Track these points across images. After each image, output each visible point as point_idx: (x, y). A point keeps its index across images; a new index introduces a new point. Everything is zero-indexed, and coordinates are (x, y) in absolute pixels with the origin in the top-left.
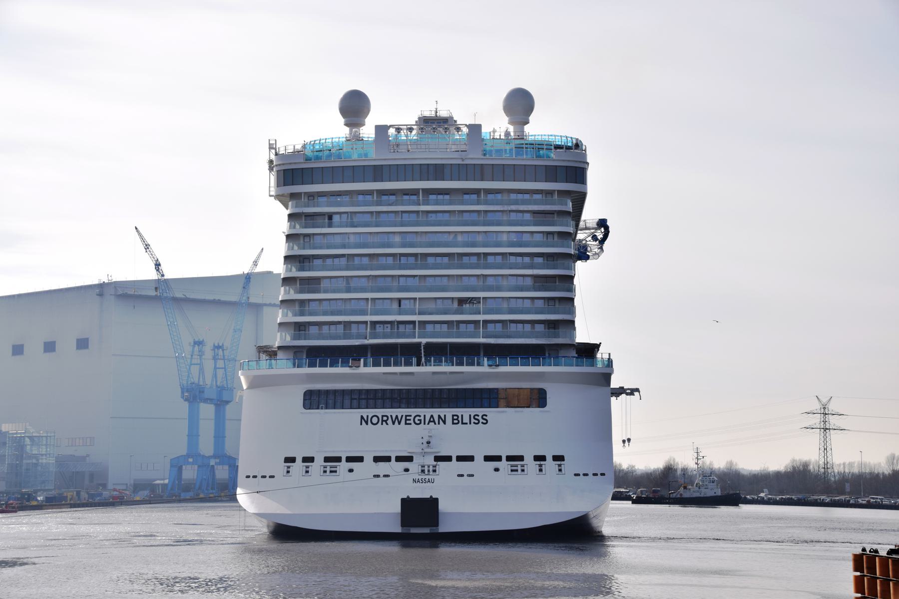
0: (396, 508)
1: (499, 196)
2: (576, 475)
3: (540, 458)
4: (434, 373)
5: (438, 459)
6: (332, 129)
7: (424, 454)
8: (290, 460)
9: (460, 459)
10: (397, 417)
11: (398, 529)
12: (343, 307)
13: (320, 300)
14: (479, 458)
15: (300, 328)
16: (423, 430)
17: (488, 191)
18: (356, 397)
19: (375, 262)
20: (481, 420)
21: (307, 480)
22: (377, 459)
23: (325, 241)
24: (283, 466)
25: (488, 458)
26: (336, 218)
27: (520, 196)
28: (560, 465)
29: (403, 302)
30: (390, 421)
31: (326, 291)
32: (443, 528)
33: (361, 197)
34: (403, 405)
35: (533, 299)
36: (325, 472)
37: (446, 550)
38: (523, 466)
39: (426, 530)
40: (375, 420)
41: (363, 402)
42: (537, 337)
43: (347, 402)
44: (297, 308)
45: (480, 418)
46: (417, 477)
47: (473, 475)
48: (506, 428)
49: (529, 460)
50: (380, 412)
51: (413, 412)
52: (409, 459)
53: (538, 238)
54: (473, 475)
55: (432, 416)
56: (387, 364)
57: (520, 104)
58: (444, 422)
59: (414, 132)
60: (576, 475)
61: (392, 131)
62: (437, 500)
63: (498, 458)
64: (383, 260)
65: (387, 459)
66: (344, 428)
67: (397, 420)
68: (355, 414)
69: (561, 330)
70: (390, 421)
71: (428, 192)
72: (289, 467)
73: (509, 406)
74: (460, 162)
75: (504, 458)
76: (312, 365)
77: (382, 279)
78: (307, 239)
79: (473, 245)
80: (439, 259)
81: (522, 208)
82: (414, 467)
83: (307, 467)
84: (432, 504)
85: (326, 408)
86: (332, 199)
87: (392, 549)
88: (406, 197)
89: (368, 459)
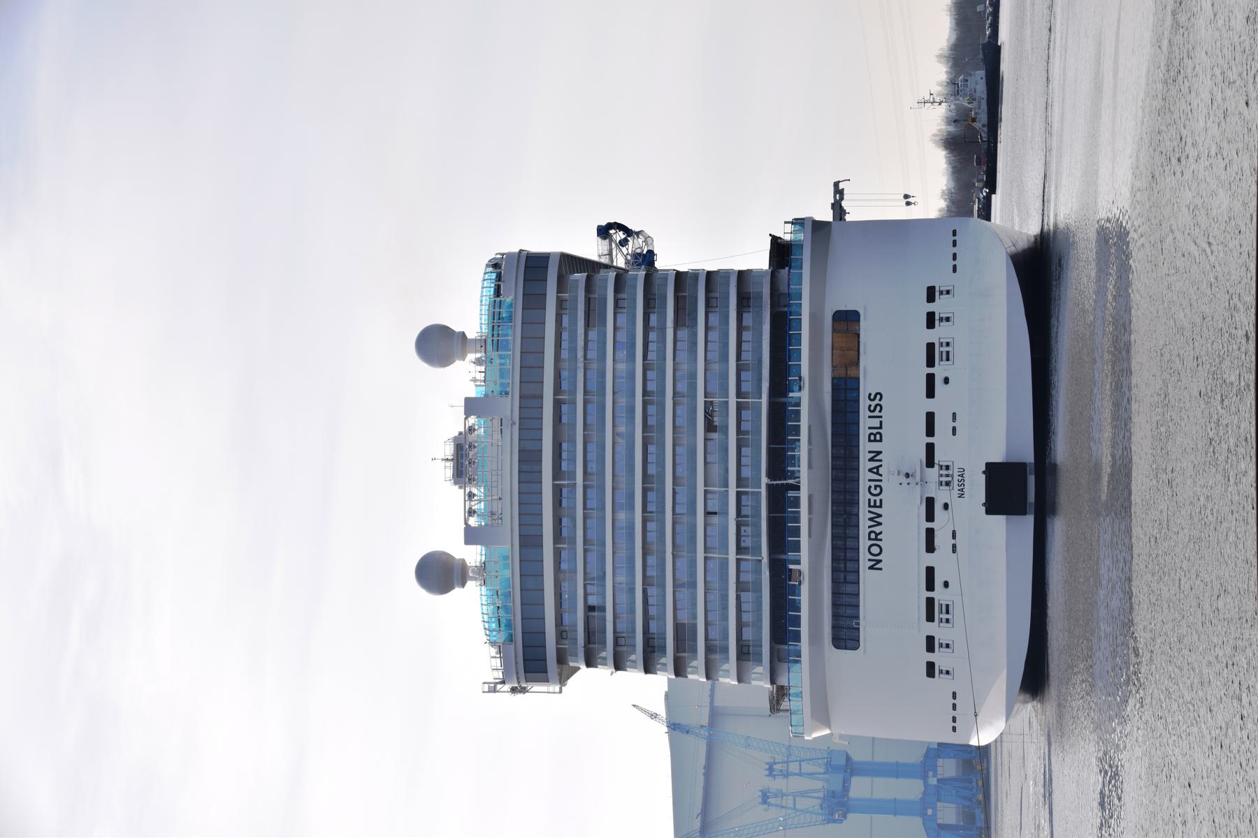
0: (1000, 520)
1: (565, 374)
2: (955, 269)
3: (931, 321)
4: (810, 467)
5: (930, 462)
6: (469, 605)
7: (924, 482)
8: (931, 669)
9: (930, 431)
10: (871, 519)
11: (1029, 521)
12: (715, 590)
13: (707, 624)
14: (930, 405)
15: (745, 653)
16: (890, 483)
17: (558, 389)
18: (842, 575)
19: (654, 548)
20: (877, 401)
21: (959, 646)
22: (930, 548)
23: (624, 616)
24: (939, 679)
25: (930, 393)
26: (593, 601)
27: (565, 345)
28: (941, 293)
29: (710, 509)
31: (694, 617)
32: (1028, 456)
33: (564, 566)
34: (855, 511)
35: (707, 329)
36: (947, 621)
37: (1061, 450)
38: (941, 344)
39: (1031, 480)
40: (875, 550)
41: (850, 566)
42: (761, 323)
43: (849, 588)
44: (717, 656)
45: (873, 404)
46: (956, 492)
47: (954, 415)
48: (888, 367)
49: (933, 336)
50: (864, 543)
51: (864, 496)
52: (930, 502)
53: (622, 320)
54: (954, 415)
55: (870, 470)
56: (797, 532)
57: (437, 344)
58: (879, 453)
59: (475, 491)
60: (955, 269)
61: (473, 522)
62: (988, 465)
63: (930, 379)
64: (652, 537)
65: (930, 533)
66: (887, 594)
67: (876, 520)
68: (867, 578)
69: (752, 289)
71: (557, 473)
72: (941, 672)
73: (857, 364)
75: (931, 370)
76: (797, 636)
77: (678, 537)
78: (622, 641)
79: (632, 410)
80: (651, 458)
81: (581, 343)
82: (941, 496)
83: (941, 645)
84: (993, 471)
85: (858, 617)
86: (565, 605)
87: (1058, 529)
88: (564, 503)
89: (930, 560)
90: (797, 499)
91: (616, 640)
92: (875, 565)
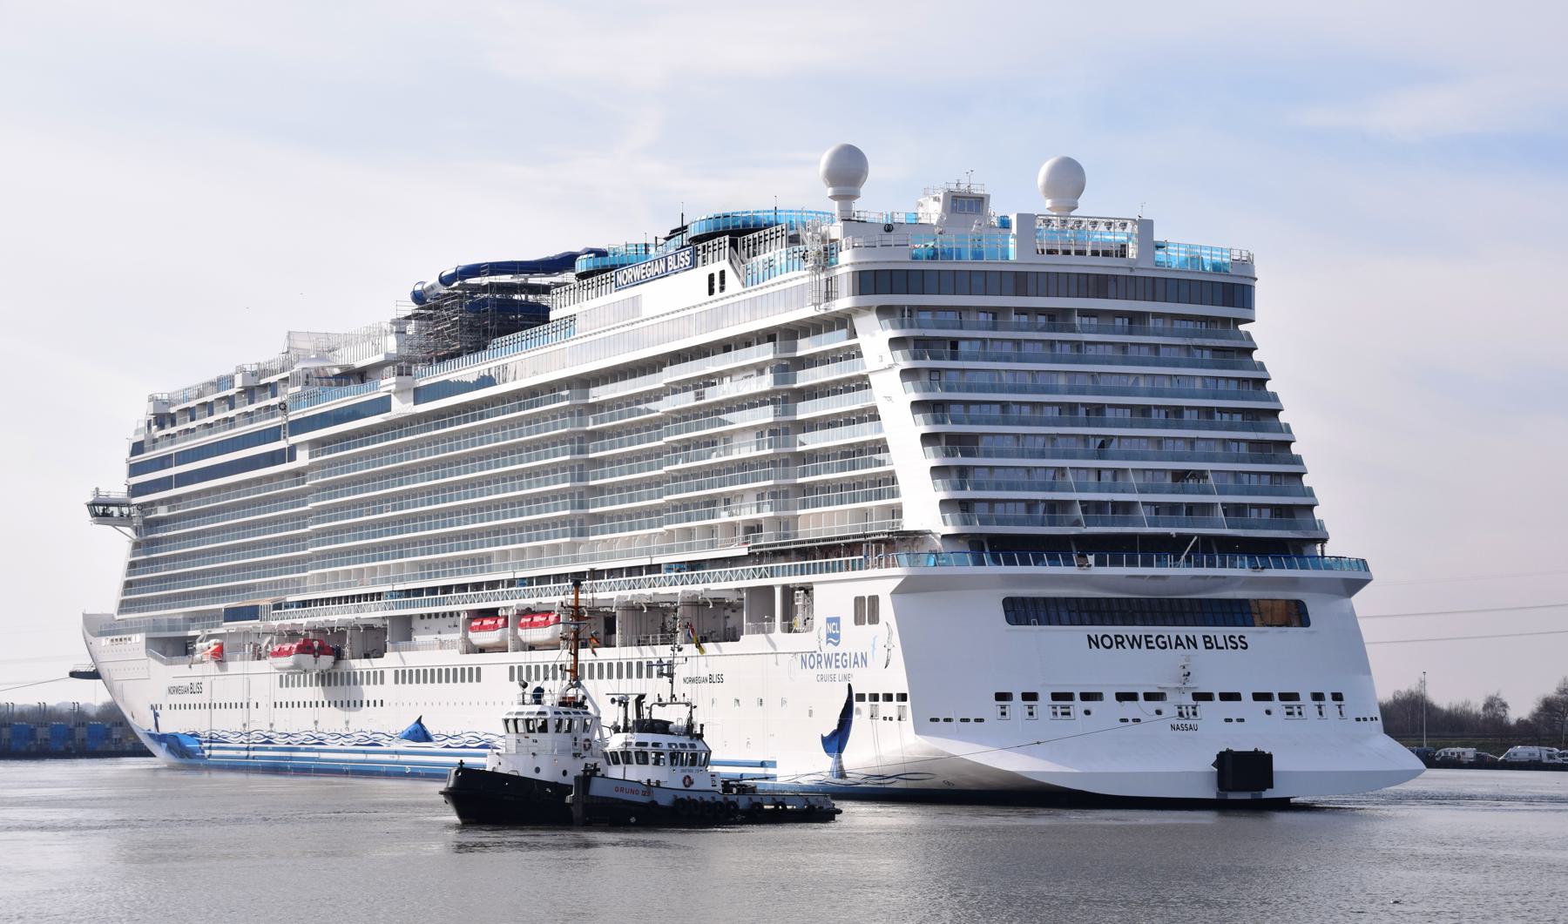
0: (1205, 763)
3: (1318, 697)
5: (1198, 697)
8: (1002, 697)
9: (1226, 697)
11: (1210, 793)
14: (1247, 697)
15: (964, 506)
17: (1157, 315)
22: (1121, 697)
25: (1258, 697)
26: (963, 347)
29: (1103, 473)
30: (1126, 643)
31: (988, 454)
32: (1268, 794)
33: (982, 317)
39: (1247, 796)
40: (1107, 642)
43: (1064, 615)
44: (955, 479)
46: (1176, 722)
48: (1267, 655)
49: (1306, 699)
50: (1112, 630)
51: (1154, 630)
57: (1068, 179)
61: (1039, 221)
63: (1266, 697)
65: (1132, 697)
66: (1065, 653)
67: (1135, 642)
70: (1126, 643)
71: (1084, 313)
74: (1127, 273)
75: (1276, 696)
76: (997, 562)
82: (1169, 708)
87: (1207, 818)
89: (1109, 697)
90: (1213, 565)
91: (937, 370)
92: (1093, 642)
